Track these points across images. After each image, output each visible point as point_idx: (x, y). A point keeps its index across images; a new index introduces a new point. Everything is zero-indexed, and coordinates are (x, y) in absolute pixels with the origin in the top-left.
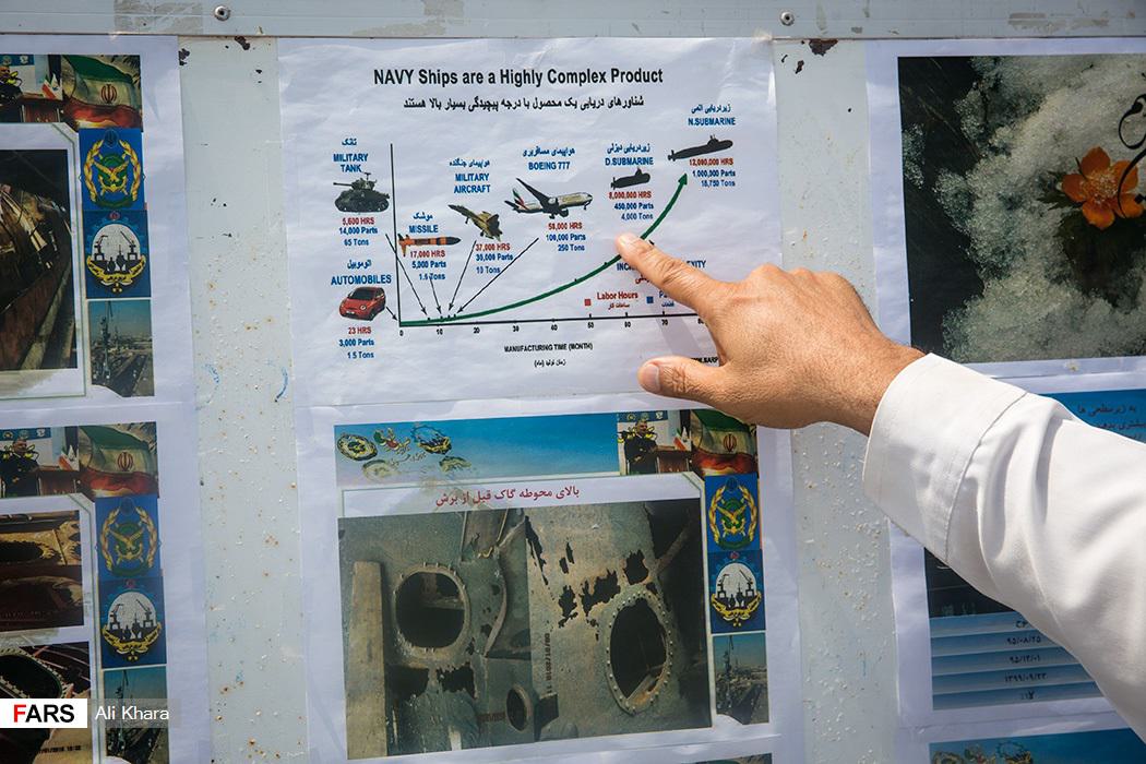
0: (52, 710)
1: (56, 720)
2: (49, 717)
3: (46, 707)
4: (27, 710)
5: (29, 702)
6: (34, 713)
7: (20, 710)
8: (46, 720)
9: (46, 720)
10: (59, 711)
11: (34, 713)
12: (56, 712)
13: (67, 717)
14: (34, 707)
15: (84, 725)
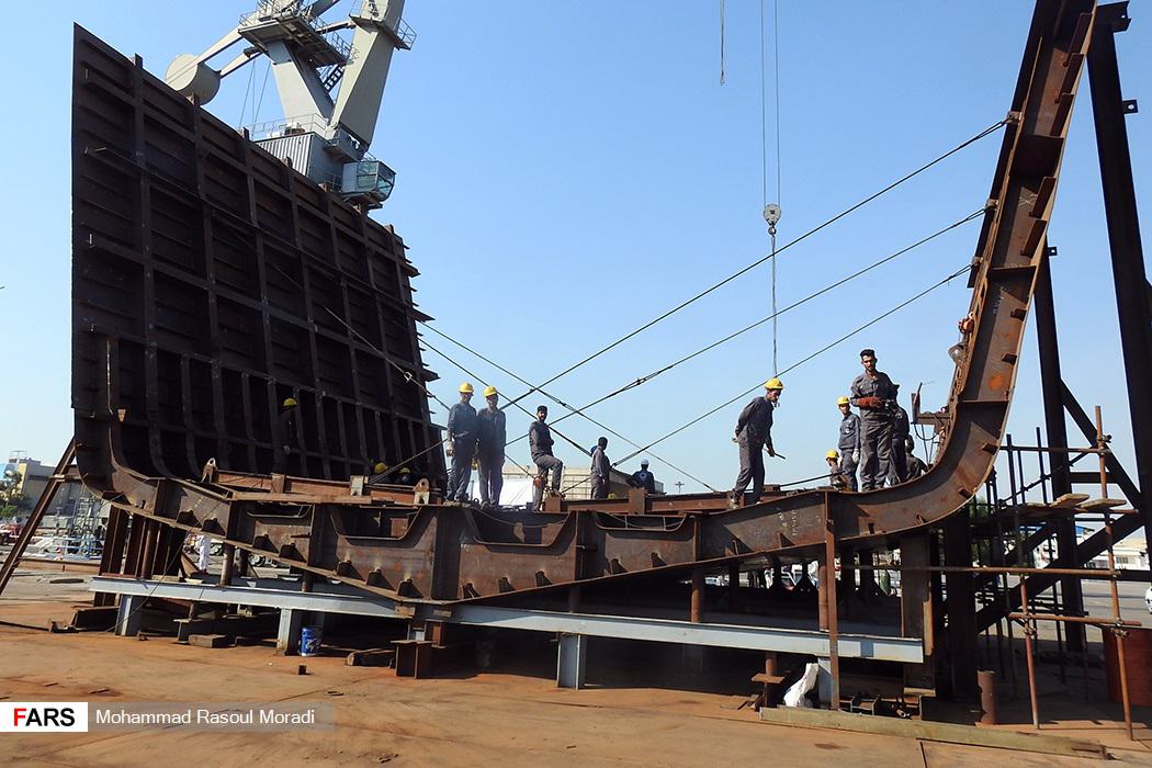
0: (53, 713)
1: (57, 724)
2: (50, 720)
3: (46, 710)
4: (27, 714)
5: (29, 706)
6: (34, 717)
7: (20, 713)
8: (46, 724)
9: (46, 724)
10: (60, 715)
11: (34, 717)
12: (56, 715)
13: (68, 721)
14: (34, 711)
15: (85, 729)
